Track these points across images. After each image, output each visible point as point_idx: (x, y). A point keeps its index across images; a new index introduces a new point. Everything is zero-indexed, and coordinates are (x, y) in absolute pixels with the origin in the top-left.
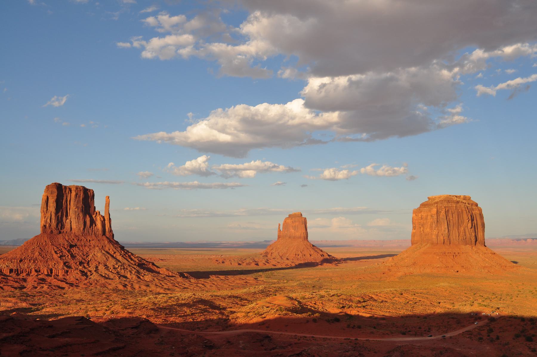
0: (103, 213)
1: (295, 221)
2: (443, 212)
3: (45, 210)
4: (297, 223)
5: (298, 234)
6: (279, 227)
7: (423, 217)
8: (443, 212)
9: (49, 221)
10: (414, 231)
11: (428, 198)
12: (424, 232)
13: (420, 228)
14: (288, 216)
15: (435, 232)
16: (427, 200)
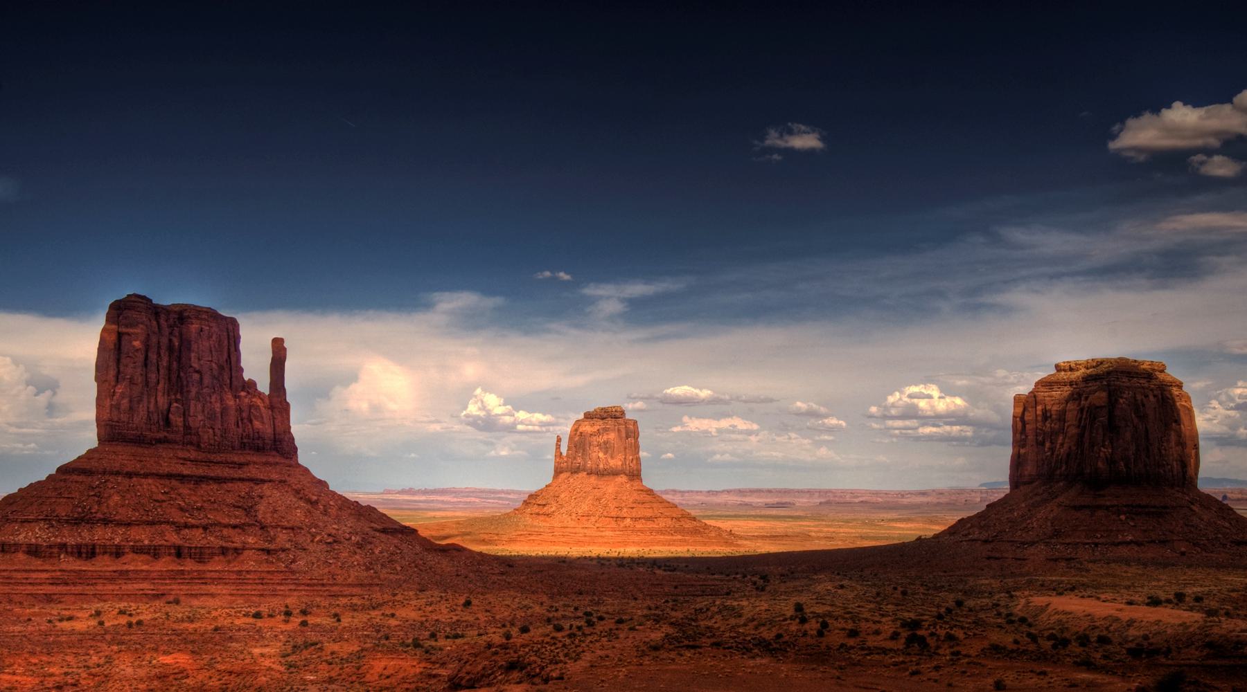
0: (264, 386)
1: (606, 430)
2: (1121, 401)
3: (112, 373)
4: (612, 436)
5: (616, 463)
6: (558, 446)
7: (1051, 415)
8: (1121, 401)
9: (125, 401)
10: (1022, 451)
11: (1057, 367)
12: (1053, 454)
13: (1043, 444)
14: (581, 416)
15: (1106, 451)
16: (1053, 371)
